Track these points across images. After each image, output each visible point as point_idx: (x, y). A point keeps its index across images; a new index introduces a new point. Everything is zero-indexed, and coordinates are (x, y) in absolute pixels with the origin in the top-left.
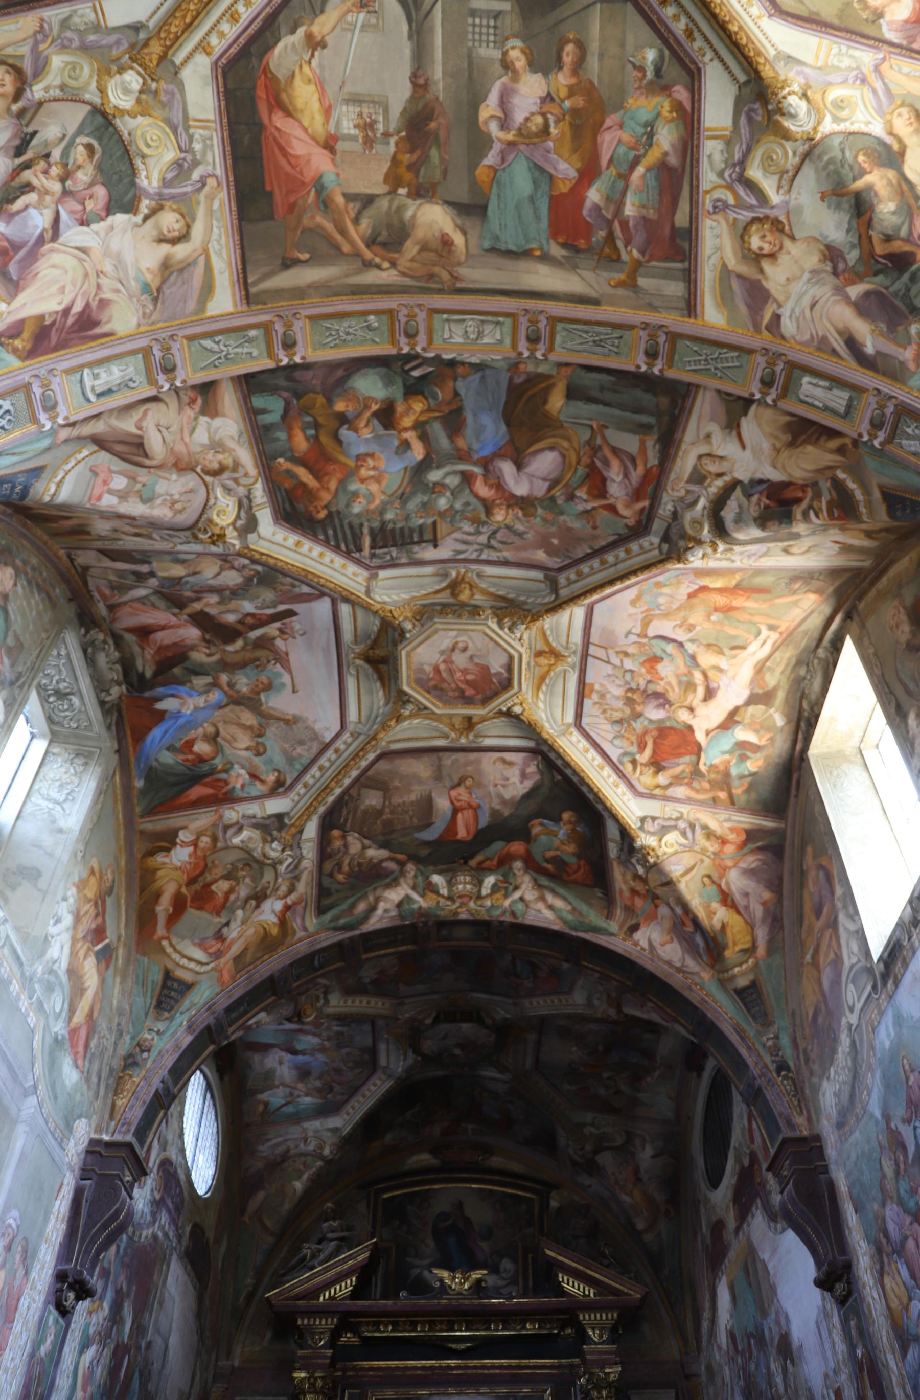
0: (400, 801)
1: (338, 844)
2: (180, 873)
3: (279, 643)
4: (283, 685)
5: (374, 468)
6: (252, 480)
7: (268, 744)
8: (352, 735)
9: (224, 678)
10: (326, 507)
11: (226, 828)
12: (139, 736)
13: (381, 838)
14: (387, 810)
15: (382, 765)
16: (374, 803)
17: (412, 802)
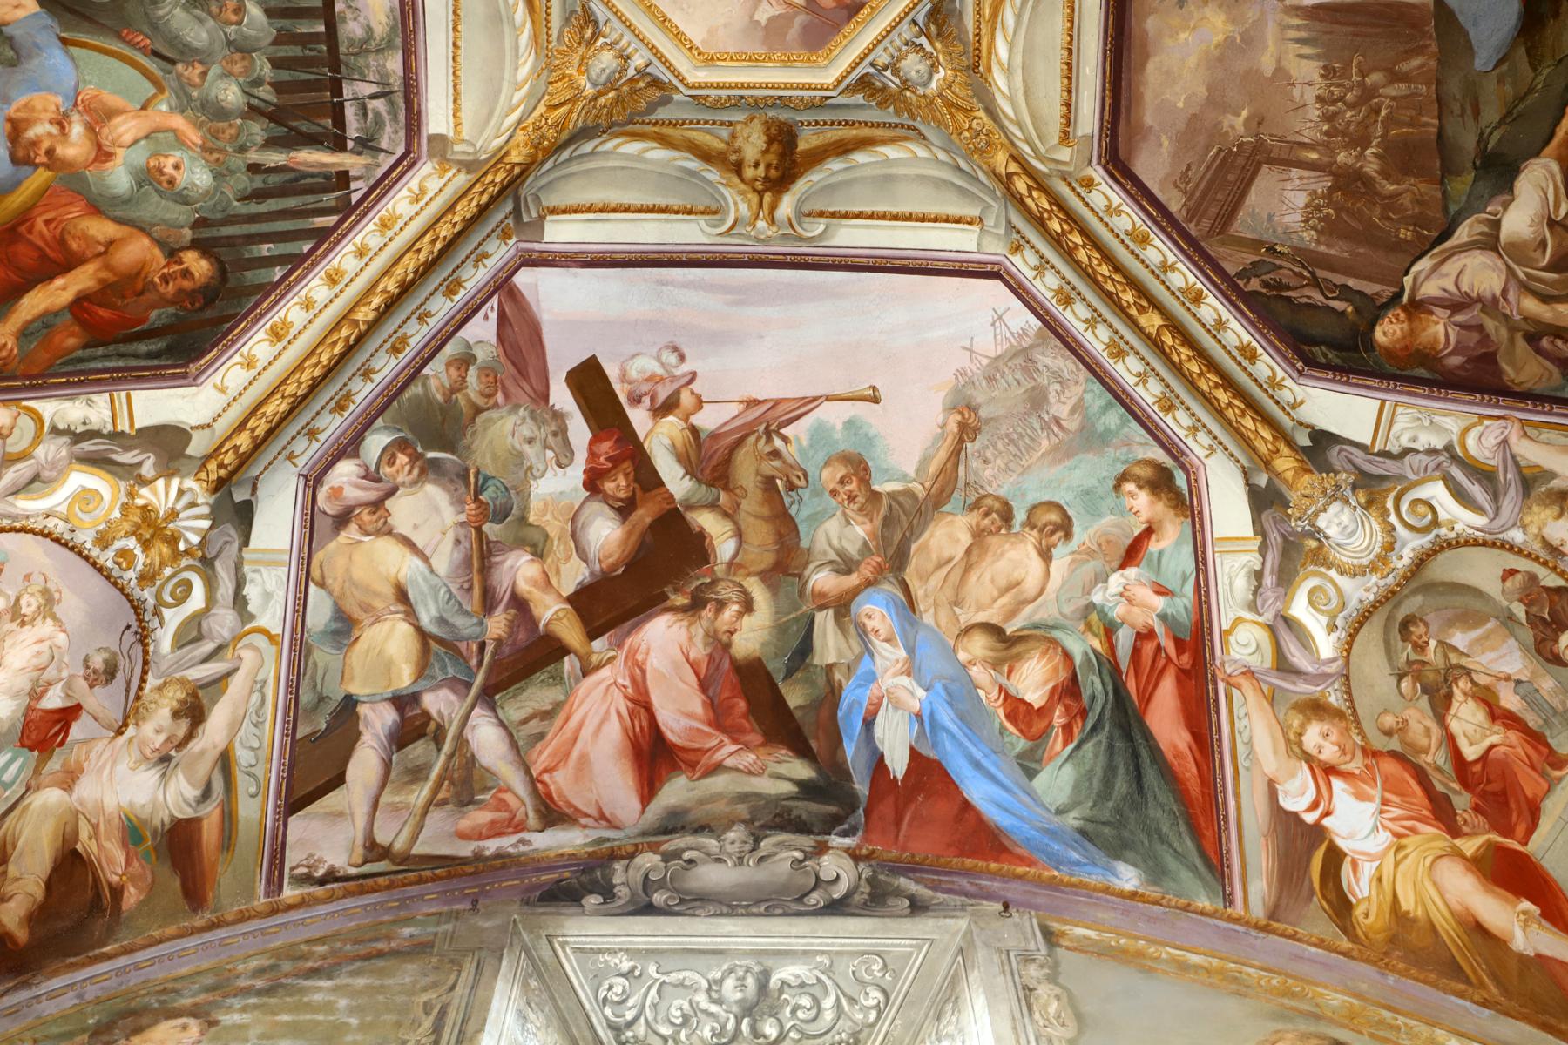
0: (1315, 113)
1: (1439, 330)
2: (1411, 841)
3: (708, 420)
4: (850, 424)
5: (61, 123)
6: (26, 423)
7: (1034, 497)
8: (1017, 249)
9: (822, 580)
10: (172, 254)
11: (1283, 665)
12: (982, 840)
13: (1461, 186)
14: (1342, 157)
15: (1153, 166)
16: (1301, 199)
17: (1328, 72)
